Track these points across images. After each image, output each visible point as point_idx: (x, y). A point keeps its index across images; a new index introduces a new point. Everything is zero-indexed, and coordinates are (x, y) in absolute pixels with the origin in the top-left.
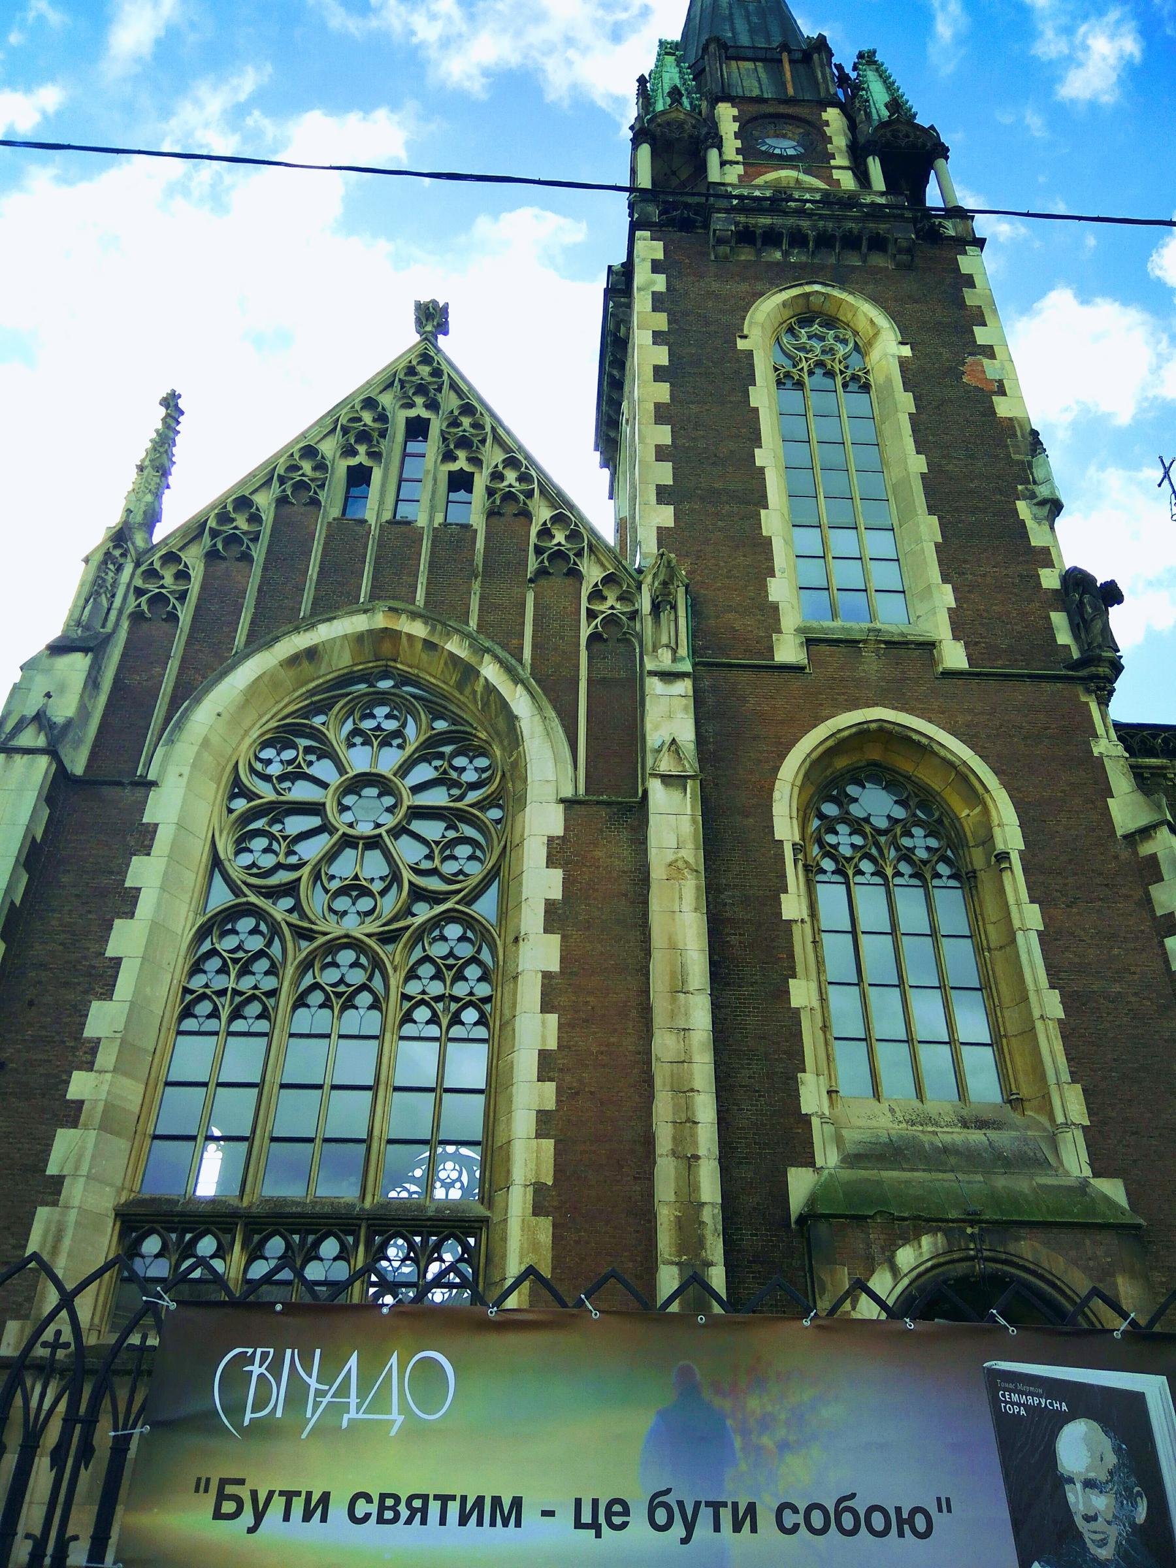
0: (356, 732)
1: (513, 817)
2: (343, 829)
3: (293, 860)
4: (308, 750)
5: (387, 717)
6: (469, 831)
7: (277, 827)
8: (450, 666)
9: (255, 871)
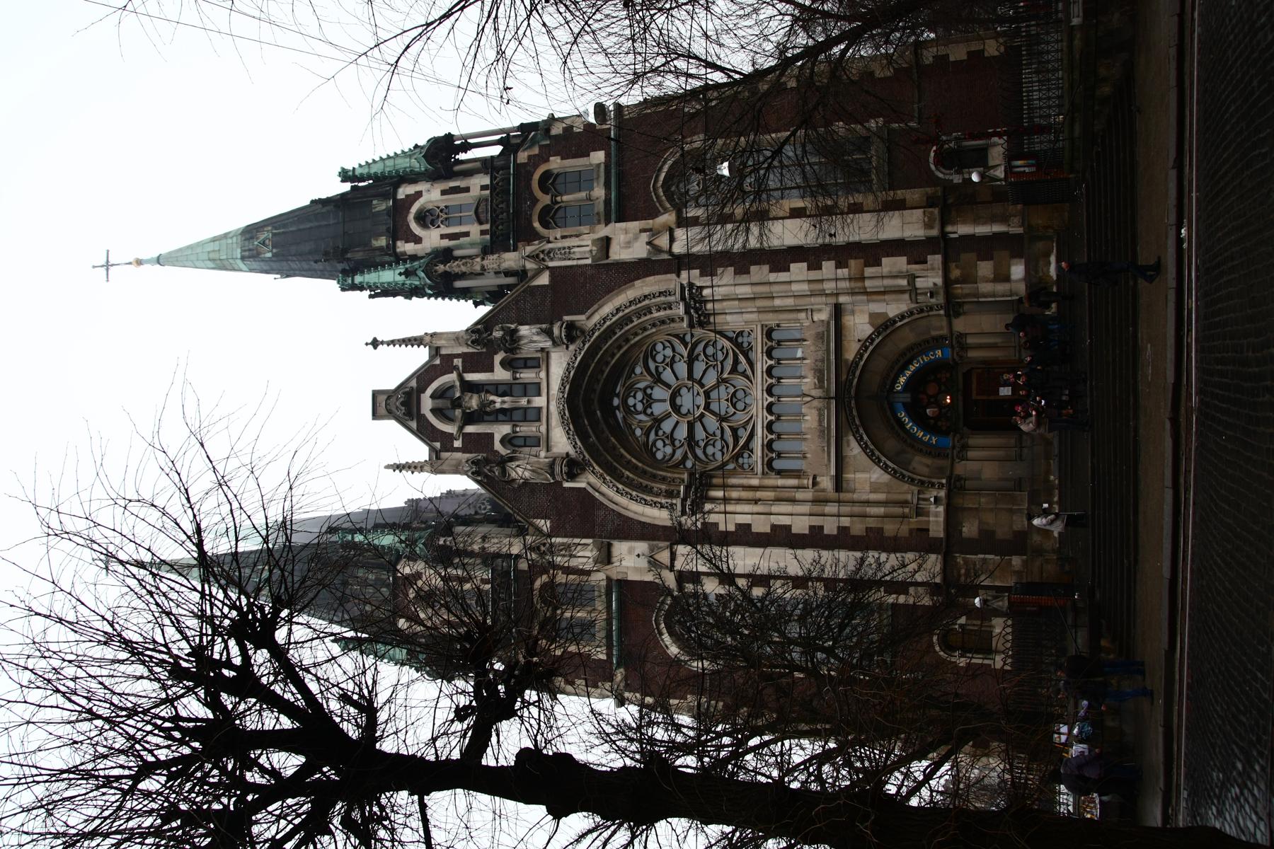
0: (644, 412)
2: (701, 410)
3: (718, 433)
4: (657, 434)
5: (634, 397)
6: (700, 347)
7: (702, 444)
9: (725, 450)
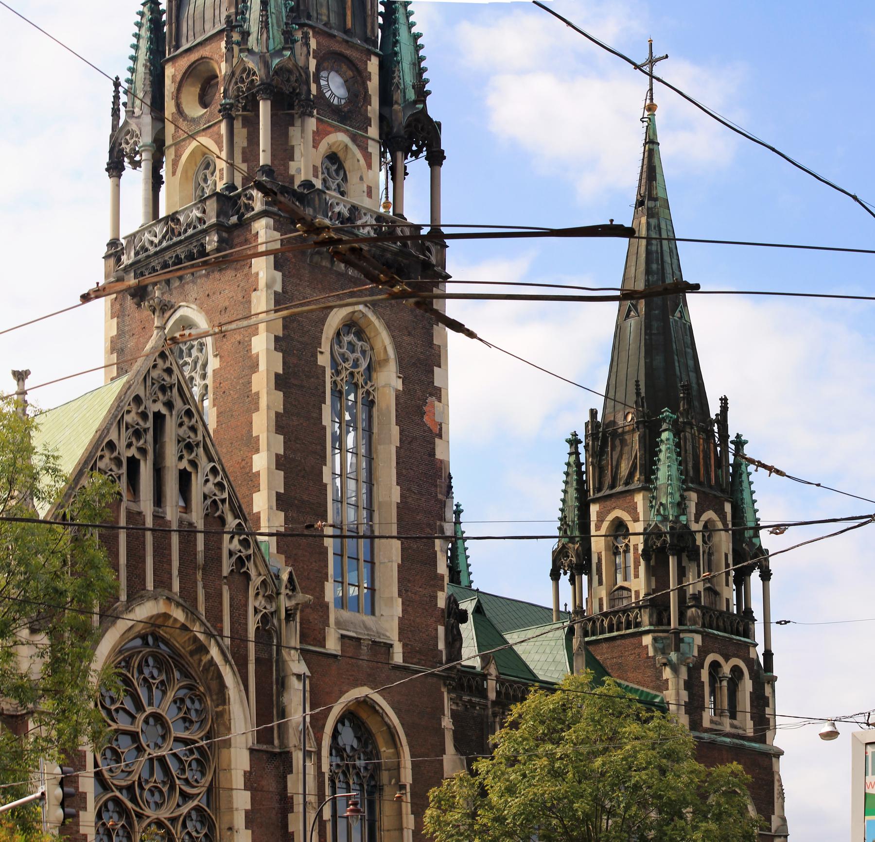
1: (219, 749)
8: (191, 642)
